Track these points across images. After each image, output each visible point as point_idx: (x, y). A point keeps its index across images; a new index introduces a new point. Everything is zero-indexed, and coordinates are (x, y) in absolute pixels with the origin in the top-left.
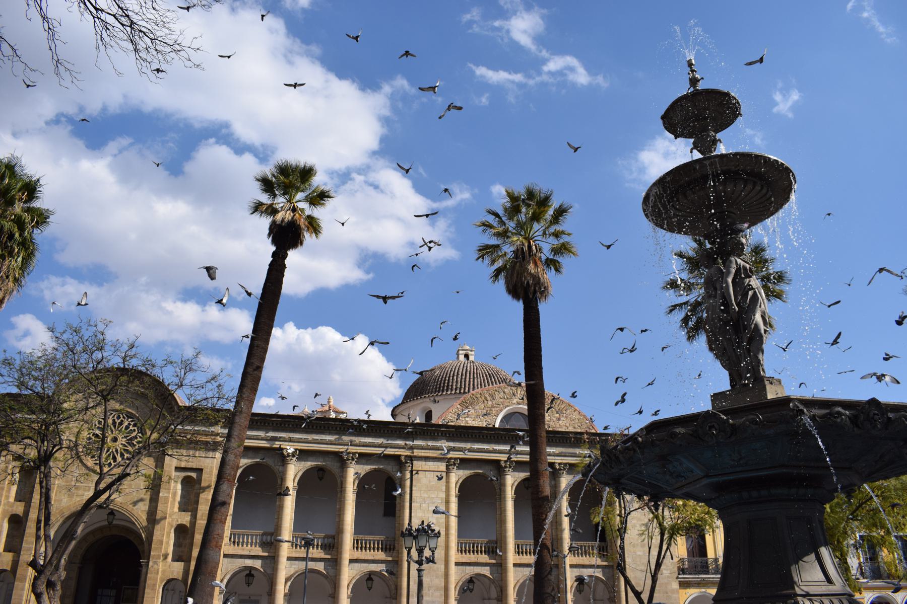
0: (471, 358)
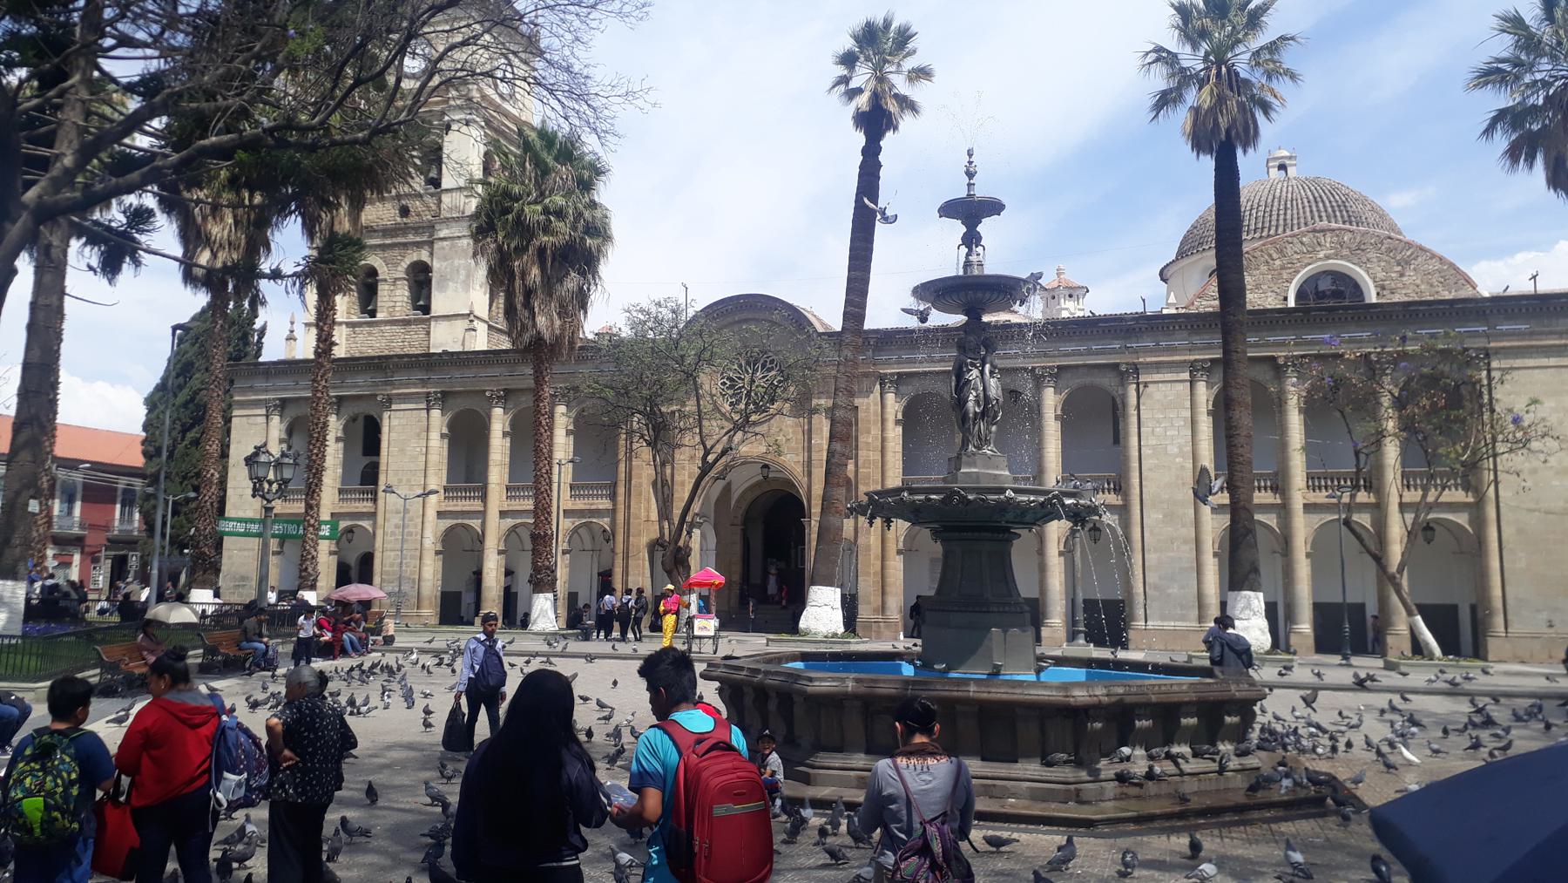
0: (1292, 171)
